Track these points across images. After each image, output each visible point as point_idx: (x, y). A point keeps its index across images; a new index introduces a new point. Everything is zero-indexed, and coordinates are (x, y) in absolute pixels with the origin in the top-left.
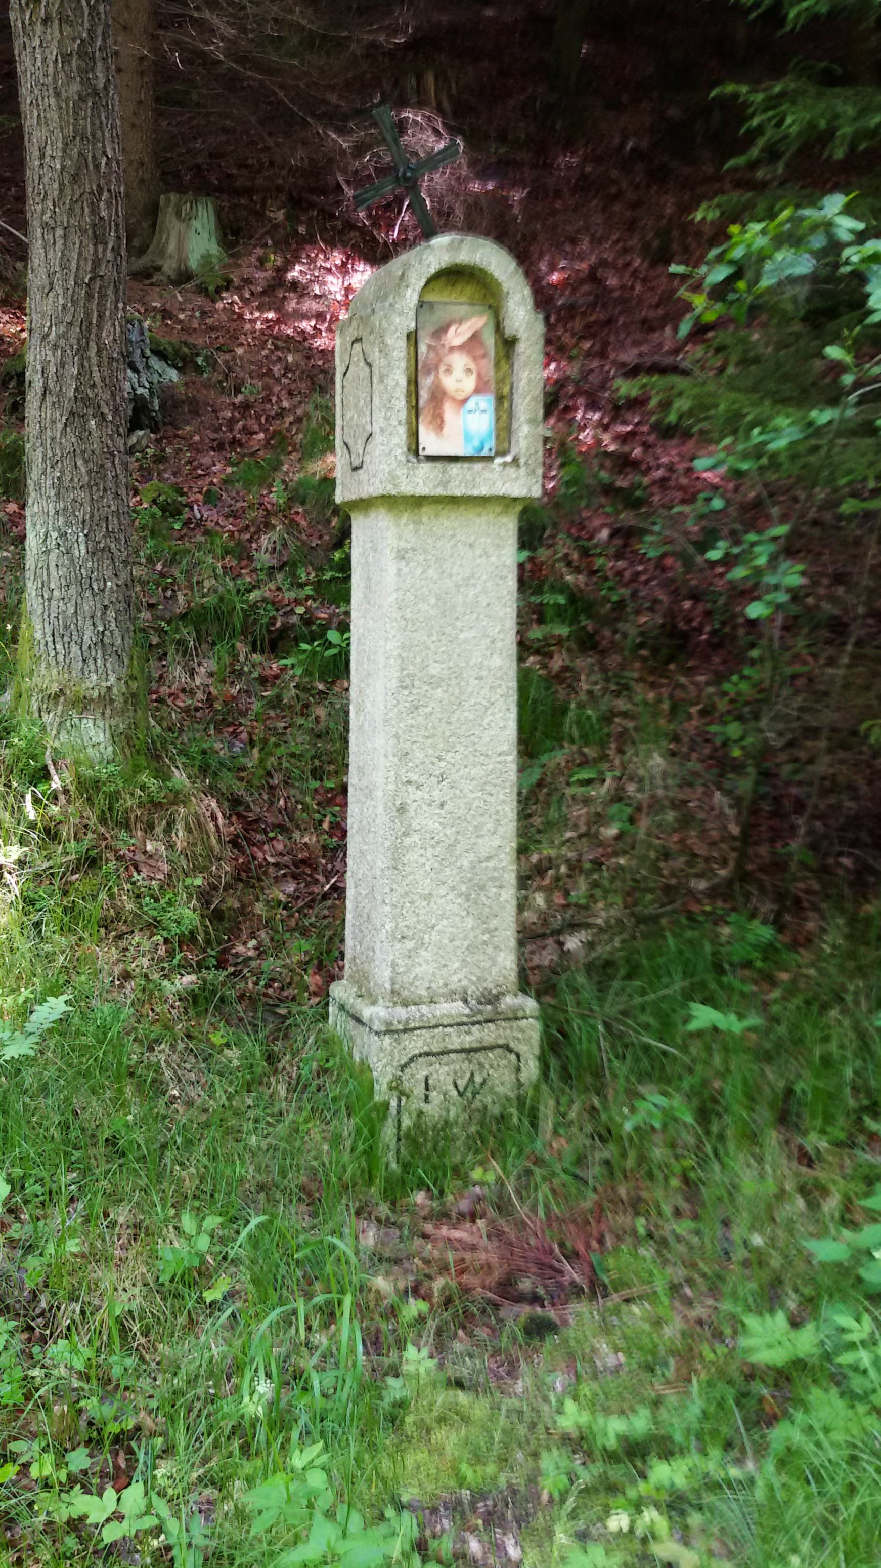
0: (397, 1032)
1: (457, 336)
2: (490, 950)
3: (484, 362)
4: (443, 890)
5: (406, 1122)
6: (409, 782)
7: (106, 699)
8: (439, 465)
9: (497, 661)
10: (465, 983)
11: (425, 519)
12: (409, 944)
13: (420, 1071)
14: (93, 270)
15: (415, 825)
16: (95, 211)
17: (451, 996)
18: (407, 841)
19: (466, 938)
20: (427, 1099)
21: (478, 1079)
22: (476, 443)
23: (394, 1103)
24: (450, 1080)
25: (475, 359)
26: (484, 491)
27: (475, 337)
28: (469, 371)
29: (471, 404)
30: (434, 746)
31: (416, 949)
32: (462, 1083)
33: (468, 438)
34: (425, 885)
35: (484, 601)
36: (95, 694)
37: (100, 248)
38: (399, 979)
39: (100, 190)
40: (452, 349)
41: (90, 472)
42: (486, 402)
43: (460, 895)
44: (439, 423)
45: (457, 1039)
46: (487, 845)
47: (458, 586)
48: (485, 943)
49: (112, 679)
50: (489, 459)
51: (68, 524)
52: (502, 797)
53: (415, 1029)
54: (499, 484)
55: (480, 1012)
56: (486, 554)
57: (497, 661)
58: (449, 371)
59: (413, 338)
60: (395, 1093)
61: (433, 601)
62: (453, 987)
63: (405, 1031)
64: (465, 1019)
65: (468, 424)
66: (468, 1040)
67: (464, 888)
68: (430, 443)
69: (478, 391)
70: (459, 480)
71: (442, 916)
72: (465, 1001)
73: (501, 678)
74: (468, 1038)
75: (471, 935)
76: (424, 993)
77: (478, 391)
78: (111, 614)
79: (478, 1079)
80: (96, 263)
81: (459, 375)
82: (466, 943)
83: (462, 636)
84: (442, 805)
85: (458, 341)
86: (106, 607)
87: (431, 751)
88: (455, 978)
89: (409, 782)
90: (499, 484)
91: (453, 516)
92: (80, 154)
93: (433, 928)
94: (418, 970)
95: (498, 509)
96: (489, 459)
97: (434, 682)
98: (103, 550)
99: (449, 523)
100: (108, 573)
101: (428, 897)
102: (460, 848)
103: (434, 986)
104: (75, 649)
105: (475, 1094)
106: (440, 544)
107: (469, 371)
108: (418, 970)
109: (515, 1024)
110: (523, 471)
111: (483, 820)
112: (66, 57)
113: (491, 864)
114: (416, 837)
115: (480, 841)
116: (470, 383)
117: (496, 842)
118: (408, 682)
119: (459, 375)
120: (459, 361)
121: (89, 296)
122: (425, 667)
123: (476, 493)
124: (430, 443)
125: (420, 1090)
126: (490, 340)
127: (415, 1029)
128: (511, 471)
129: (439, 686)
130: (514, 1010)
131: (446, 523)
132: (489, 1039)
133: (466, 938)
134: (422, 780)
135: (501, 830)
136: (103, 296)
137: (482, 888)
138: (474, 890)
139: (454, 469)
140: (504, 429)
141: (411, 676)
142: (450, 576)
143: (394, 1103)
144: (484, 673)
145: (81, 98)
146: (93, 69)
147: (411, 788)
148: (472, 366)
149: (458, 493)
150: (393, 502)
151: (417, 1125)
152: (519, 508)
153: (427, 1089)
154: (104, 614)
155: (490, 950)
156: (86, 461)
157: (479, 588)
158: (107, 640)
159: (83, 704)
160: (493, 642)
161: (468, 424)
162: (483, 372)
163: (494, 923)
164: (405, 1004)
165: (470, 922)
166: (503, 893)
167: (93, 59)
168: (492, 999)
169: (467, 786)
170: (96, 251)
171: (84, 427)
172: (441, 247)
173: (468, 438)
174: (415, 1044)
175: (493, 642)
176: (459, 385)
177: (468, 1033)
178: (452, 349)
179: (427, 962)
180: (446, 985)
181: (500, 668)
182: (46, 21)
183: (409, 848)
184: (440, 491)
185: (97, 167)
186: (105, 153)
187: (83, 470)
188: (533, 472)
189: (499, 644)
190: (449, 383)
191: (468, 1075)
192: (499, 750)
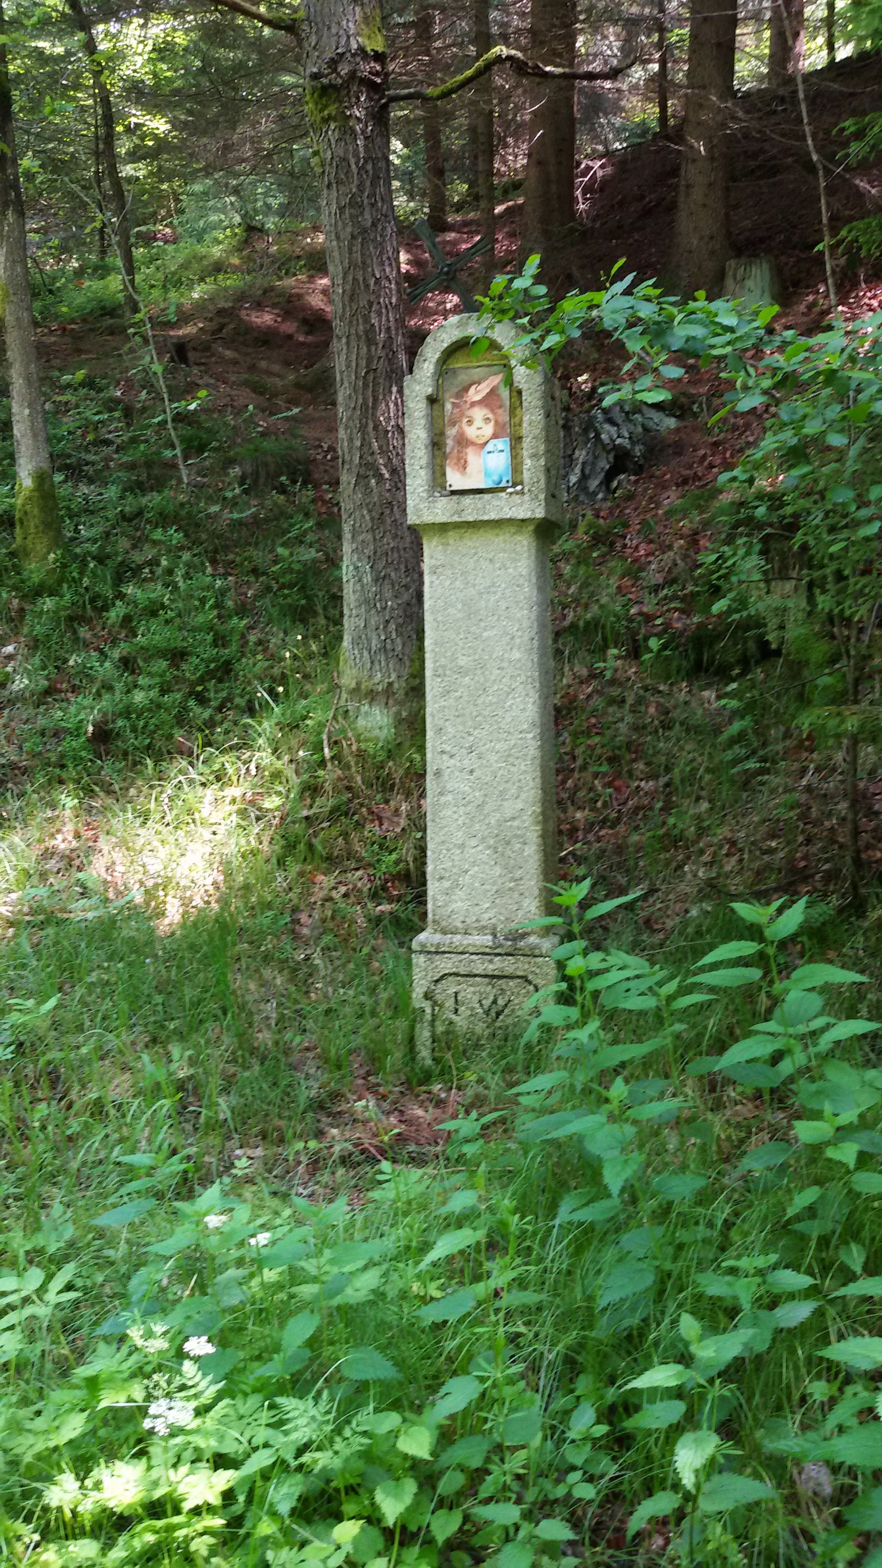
0: (429, 952)
1: (476, 394)
2: (516, 895)
3: (500, 411)
4: (474, 842)
5: (440, 1029)
6: (443, 752)
7: (389, 690)
8: (455, 497)
9: (516, 655)
10: (493, 921)
11: (451, 542)
12: (446, 884)
13: (451, 987)
14: (367, 366)
15: (449, 787)
16: (367, 319)
17: (482, 930)
18: (443, 799)
19: (494, 883)
20: (456, 1011)
21: (501, 1002)
22: (496, 478)
23: (428, 1010)
24: (476, 998)
25: (492, 411)
26: (493, 516)
27: (493, 392)
28: (487, 420)
29: (490, 447)
30: (464, 724)
31: (451, 888)
32: (487, 1003)
33: (487, 474)
34: (459, 836)
35: (503, 605)
36: (380, 688)
37: (373, 348)
38: (438, 911)
39: (371, 304)
40: (473, 404)
41: (372, 519)
42: (503, 444)
43: (489, 847)
44: (463, 466)
45: (480, 966)
46: (511, 807)
47: (481, 594)
48: (510, 889)
49: (393, 677)
50: (503, 489)
51: (359, 559)
52: (523, 768)
53: (444, 953)
54: (506, 509)
55: (501, 946)
56: (504, 567)
57: (516, 655)
58: (470, 422)
59: (432, 400)
60: (429, 1003)
61: (460, 606)
62: (483, 923)
63: (437, 953)
64: (488, 950)
65: (487, 464)
66: (490, 968)
67: (492, 842)
68: (455, 479)
69: (495, 436)
70: (471, 509)
71: (474, 864)
72: (495, 936)
73: (520, 669)
74: (491, 967)
75: (500, 881)
76: (459, 925)
77: (495, 436)
78: (392, 626)
79: (501, 1002)
80: (369, 360)
81: (479, 424)
82: (495, 888)
83: (485, 634)
84: (472, 772)
85: (478, 398)
86: (387, 622)
87: (461, 728)
88: (486, 916)
89: (443, 752)
90: (506, 509)
91: (475, 537)
92: (354, 279)
93: (466, 872)
94: (454, 906)
95: (513, 530)
96: (503, 489)
97: (462, 671)
98: (384, 578)
99: (472, 542)
100: (388, 594)
101: (462, 846)
102: (487, 809)
103: (468, 921)
104: (366, 653)
105: (498, 1014)
106: (465, 560)
107: (487, 420)
108: (454, 906)
109: (533, 960)
110: (526, 497)
111: (508, 786)
112: (341, 209)
113: (516, 823)
114: (450, 797)
115: (505, 804)
116: (488, 430)
117: (520, 806)
118: (440, 671)
119: (479, 424)
120: (479, 414)
121: (366, 386)
122: (454, 659)
123: (486, 518)
124: (455, 479)
125: (450, 1003)
126: (505, 393)
127: (444, 953)
128: (517, 499)
129: (466, 675)
130: (533, 948)
131: (469, 543)
132: (509, 970)
133: (494, 883)
134: (454, 751)
135: (523, 796)
136: (376, 384)
137: (508, 843)
138: (500, 845)
139: (467, 500)
140: (516, 466)
141: (444, 667)
142: (474, 586)
143: (428, 1010)
144: (505, 664)
145: (353, 237)
146: (362, 214)
147: (445, 757)
148: (490, 416)
149: (471, 519)
150: (443, 528)
151: (447, 1033)
152: (531, 528)
153: (456, 1001)
154: (385, 627)
155: (516, 895)
156: (370, 511)
157: (499, 594)
158: (389, 647)
159: (372, 696)
160: (512, 638)
161: (487, 464)
162: (500, 420)
163: (518, 873)
164: (444, 932)
165: (498, 870)
166: (526, 848)
167: (361, 206)
168: (517, 936)
169: (493, 758)
170: (369, 351)
171: (367, 486)
172: (451, 326)
173: (487, 474)
174: (446, 965)
175: (512, 638)
176: (479, 432)
177: (491, 961)
178: (473, 404)
179: (462, 900)
180: (477, 921)
181: (519, 660)
182: (329, 186)
183: (446, 805)
184: (456, 519)
185: (367, 286)
186: (374, 275)
187: (368, 518)
188: (537, 496)
189: (518, 641)
190: (471, 432)
191: (492, 998)
192: (520, 728)
